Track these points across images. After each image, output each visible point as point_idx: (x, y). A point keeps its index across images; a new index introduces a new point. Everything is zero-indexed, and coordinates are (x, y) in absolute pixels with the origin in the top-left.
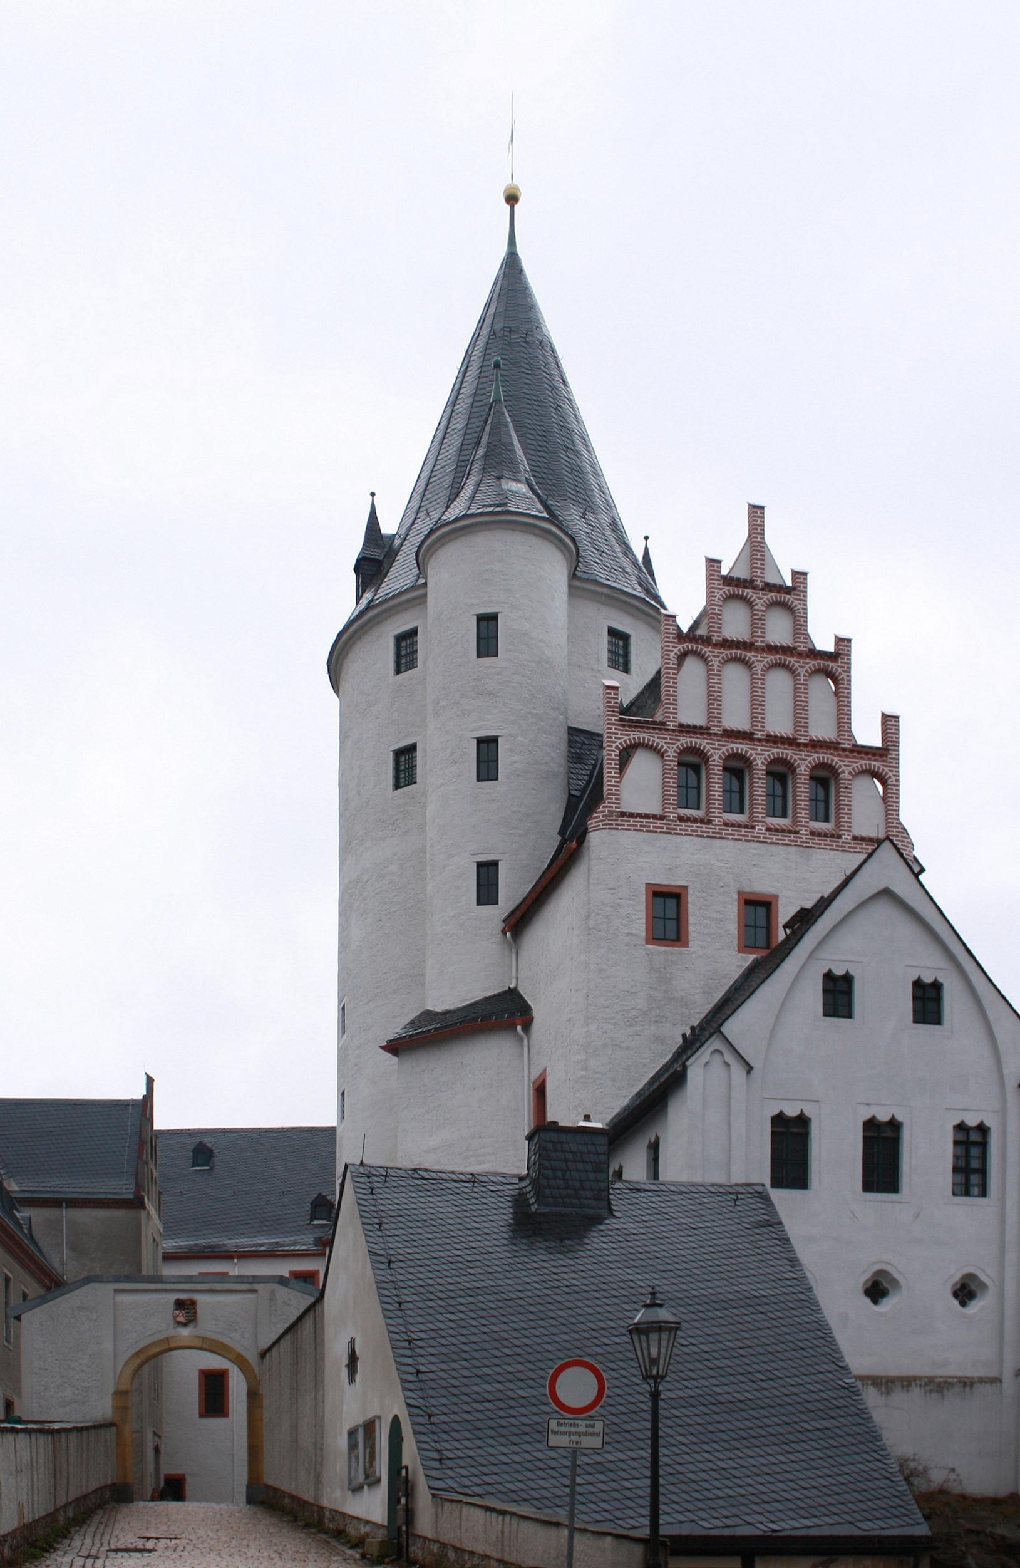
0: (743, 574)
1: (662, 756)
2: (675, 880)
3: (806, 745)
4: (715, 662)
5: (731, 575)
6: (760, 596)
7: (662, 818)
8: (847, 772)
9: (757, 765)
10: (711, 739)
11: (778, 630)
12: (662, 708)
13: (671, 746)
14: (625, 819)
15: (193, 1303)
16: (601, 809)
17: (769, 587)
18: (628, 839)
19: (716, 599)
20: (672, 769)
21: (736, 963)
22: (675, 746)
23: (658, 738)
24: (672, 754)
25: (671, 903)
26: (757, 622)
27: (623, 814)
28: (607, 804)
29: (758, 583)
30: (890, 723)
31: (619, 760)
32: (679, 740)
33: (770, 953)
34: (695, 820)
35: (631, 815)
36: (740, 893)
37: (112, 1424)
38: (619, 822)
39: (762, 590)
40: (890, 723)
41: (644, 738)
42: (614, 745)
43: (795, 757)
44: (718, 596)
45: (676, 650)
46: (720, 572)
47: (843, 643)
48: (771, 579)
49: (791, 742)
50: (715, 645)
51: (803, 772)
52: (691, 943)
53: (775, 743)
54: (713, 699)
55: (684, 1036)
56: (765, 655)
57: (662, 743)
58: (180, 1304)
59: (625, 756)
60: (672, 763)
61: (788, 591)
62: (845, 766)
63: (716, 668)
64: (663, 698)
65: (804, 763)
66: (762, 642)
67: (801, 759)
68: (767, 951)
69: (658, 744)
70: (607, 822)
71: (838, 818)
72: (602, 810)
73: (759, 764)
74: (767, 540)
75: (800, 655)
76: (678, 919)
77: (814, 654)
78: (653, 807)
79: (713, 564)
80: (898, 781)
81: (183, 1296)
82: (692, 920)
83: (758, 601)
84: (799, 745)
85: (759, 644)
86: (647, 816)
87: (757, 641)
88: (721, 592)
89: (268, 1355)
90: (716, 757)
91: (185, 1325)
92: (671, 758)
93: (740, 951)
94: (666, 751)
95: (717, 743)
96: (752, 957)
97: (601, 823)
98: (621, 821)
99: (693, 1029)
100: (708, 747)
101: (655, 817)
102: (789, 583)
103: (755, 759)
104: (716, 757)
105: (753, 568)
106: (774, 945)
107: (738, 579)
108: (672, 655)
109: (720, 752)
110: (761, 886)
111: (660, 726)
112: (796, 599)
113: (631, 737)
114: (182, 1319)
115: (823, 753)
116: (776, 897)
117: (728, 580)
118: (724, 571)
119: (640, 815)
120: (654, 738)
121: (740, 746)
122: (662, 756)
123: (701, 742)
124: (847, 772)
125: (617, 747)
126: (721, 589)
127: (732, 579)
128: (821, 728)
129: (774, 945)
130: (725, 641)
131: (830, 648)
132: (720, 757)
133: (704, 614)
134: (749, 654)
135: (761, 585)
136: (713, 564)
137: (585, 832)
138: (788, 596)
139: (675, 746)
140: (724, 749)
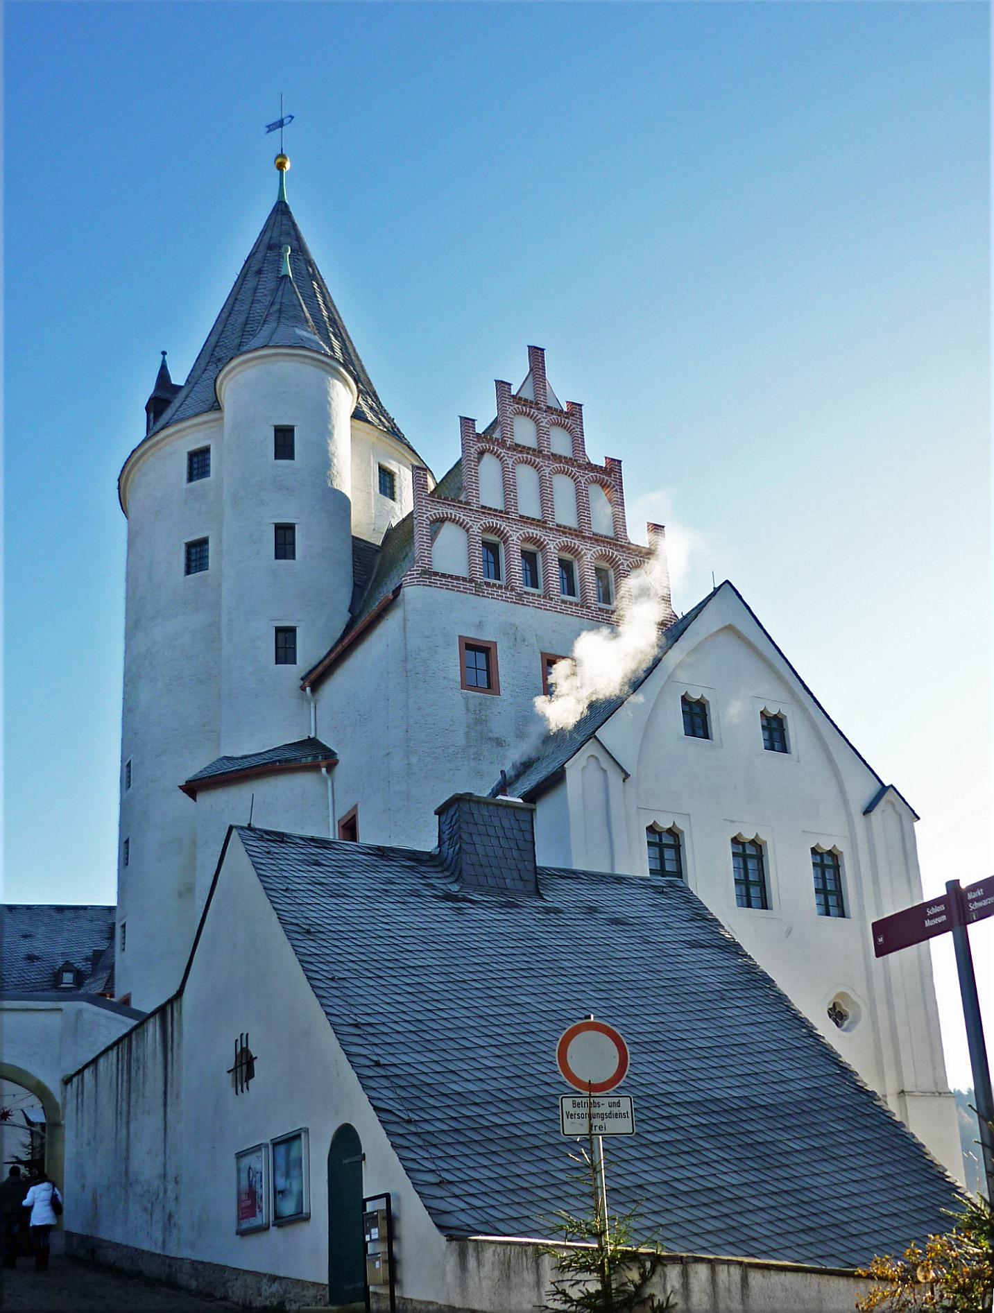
0: (528, 394)
1: (467, 531)
2: (486, 636)
4: (510, 462)
5: (519, 395)
6: (544, 416)
7: (471, 581)
8: (625, 565)
9: (550, 548)
10: (509, 523)
11: (560, 443)
12: (465, 492)
13: (475, 523)
14: (438, 578)
16: (416, 568)
19: (508, 413)
20: (477, 543)
22: (479, 524)
23: (464, 515)
24: (476, 529)
25: (481, 657)
26: (541, 433)
27: (436, 574)
28: (420, 564)
29: (542, 406)
32: (482, 520)
35: (443, 575)
36: (542, 654)
38: (432, 581)
39: (545, 412)
41: (451, 514)
42: (425, 516)
43: (581, 546)
44: (510, 410)
45: (476, 447)
46: (510, 392)
47: (614, 467)
50: (509, 449)
51: (589, 560)
52: (502, 692)
53: (564, 533)
54: (509, 488)
57: (467, 519)
60: (477, 538)
63: (510, 466)
66: (548, 451)
67: (586, 549)
69: (464, 520)
70: (421, 579)
73: (552, 548)
75: (579, 466)
76: (488, 671)
77: (591, 467)
79: (502, 386)
82: (501, 671)
83: (543, 419)
84: (584, 537)
85: (546, 453)
86: (457, 578)
87: (544, 451)
88: (512, 408)
92: (476, 533)
94: (471, 527)
95: (514, 526)
97: (416, 580)
98: (434, 579)
100: (507, 528)
101: (464, 579)
103: (548, 544)
107: (526, 400)
109: (518, 534)
112: (574, 424)
113: (440, 511)
115: (604, 546)
117: (516, 399)
118: (514, 392)
119: (451, 576)
120: (461, 515)
121: (535, 532)
122: (467, 531)
123: (502, 524)
124: (625, 565)
125: (427, 518)
126: (512, 406)
127: (520, 399)
130: (518, 445)
132: (518, 538)
133: (495, 422)
134: (538, 460)
136: (502, 386)
138: (567, 420)
139: (479, 524)
140: (521, 532)
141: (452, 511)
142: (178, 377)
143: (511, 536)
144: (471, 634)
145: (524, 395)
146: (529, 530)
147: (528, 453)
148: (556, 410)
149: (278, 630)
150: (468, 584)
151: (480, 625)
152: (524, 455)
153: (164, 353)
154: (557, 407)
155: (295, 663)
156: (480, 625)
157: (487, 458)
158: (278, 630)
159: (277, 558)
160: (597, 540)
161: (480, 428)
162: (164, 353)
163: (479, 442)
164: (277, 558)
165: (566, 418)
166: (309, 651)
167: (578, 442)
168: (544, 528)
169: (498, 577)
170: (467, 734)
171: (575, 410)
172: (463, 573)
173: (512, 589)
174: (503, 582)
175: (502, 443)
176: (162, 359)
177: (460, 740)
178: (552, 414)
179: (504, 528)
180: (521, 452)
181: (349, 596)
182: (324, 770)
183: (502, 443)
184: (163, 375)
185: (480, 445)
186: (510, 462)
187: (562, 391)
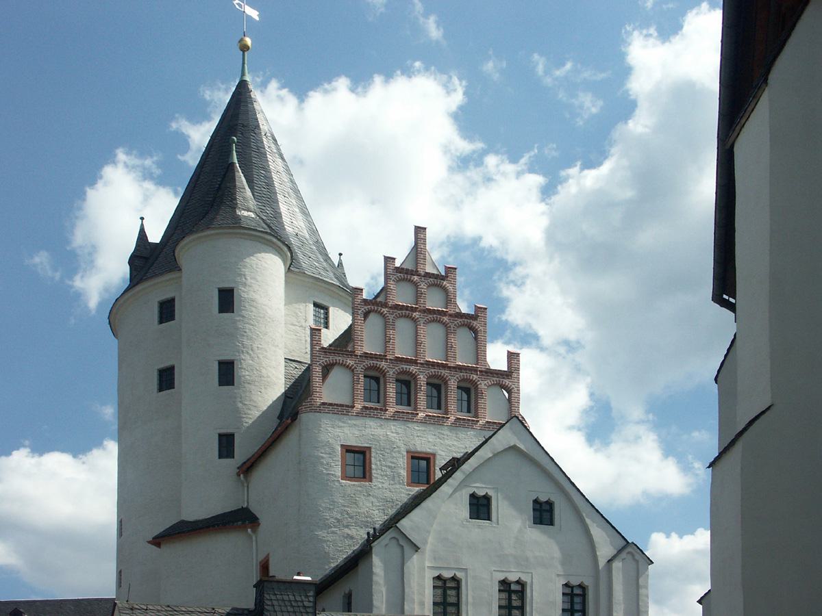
1: (353, 371)
4: (391, 317)
5: (403, 267)
11: (433, 301)
24: (359, 369)
26: (418, 295)
31: (322, 372)
34: (376, 409)
41: (339, 360)
48: (429, 269)
56: (426, 314)
61: (443, 278)
63: (391, 321)
77: (460, 315)
79: (388, 260)
86: (342, 406)
101: (347, 406)
102: (443, 274)
105: (417, 263)
107: (407, 270)
108: (360, 312)
109: (394, 370)
117: (398, 270)
118: (398, 264)
119: (337, 405)
127: (403, 269)
132: (394, 373)
135: (423, 273)
139: (362, 366)
141: (340, 358)
143: (388, 372)
146: (403, 366)
147: (407, 310)
152: (404, 312)
153: (142, 219)
157: (372, 317)
162: (142, 219)
163: (365, 305)
165: (442, 279)
167: (449, 299)
175: (385, 305)
176: (141, 223)
178: (430, 277)
179: (383, 367)
185: (366, 307)
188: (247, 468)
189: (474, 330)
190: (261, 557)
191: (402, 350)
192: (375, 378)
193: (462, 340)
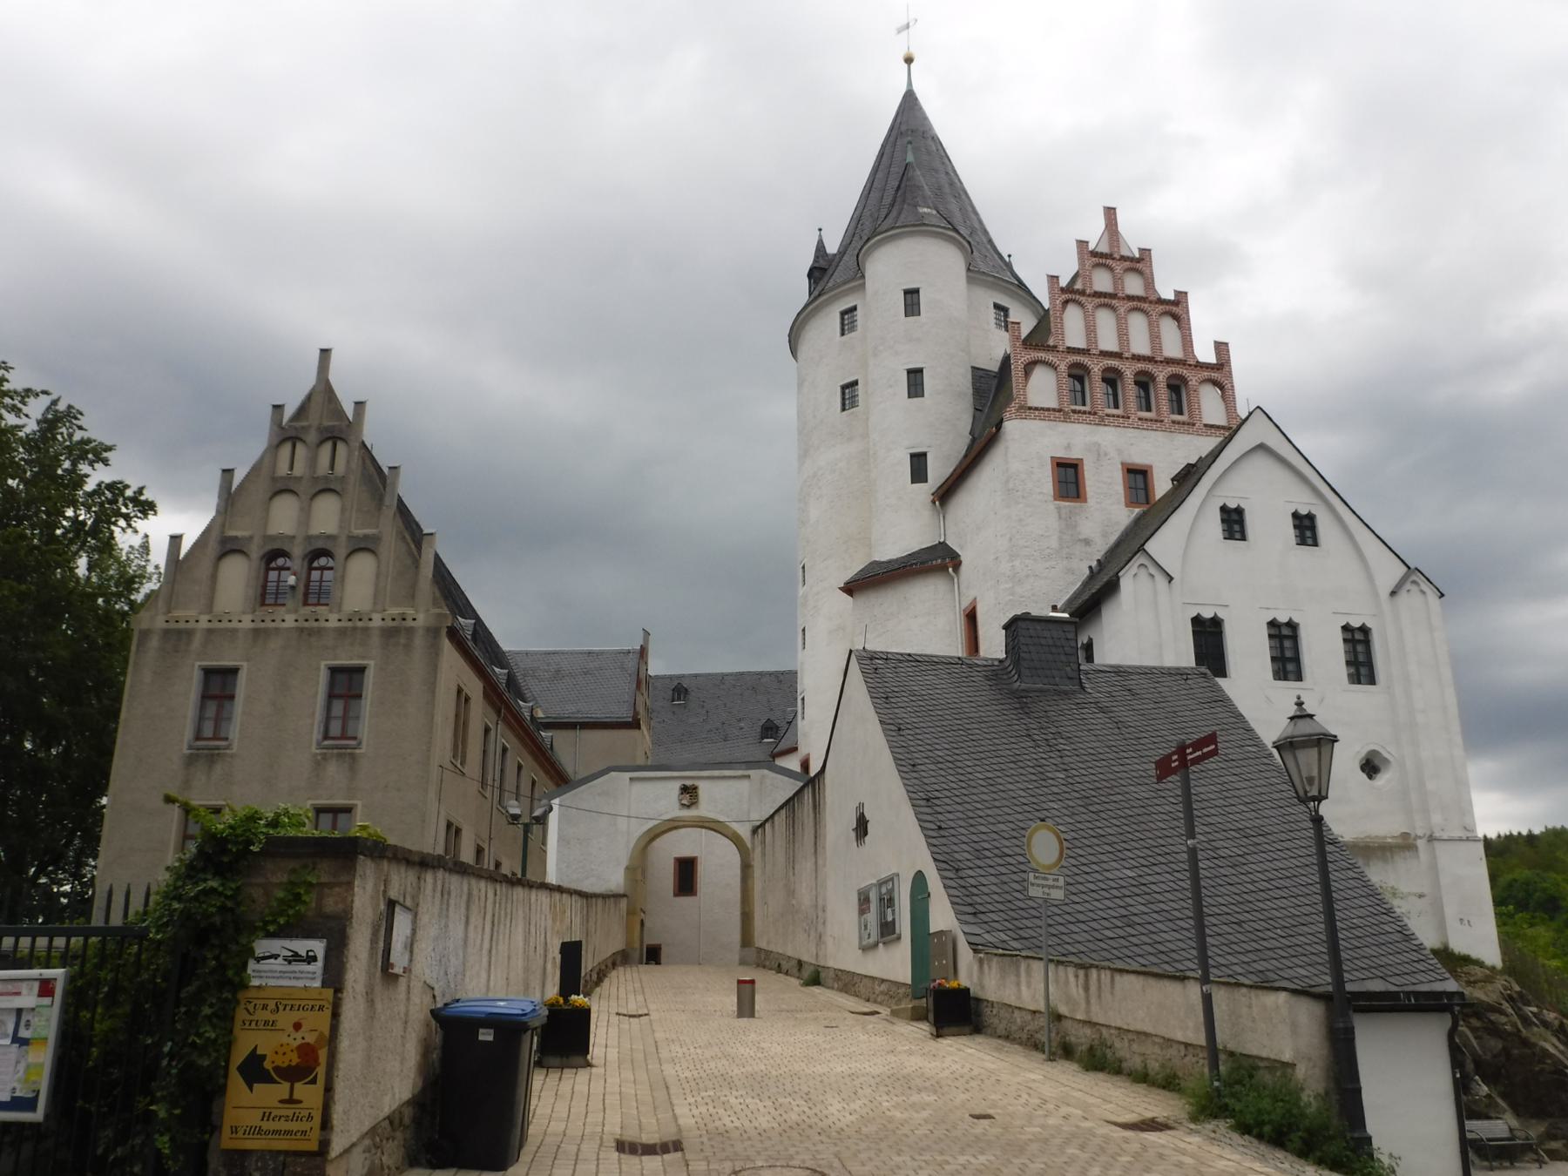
0: (1104, 249)
1: (1056, 369)
2: (1074, 455)
3: (1161, 362)
4: (1090, 307)
7: (1060, 410)
11: (1134, 286)
15: (695, 788)
17: (1123, 258)
18: (1033, 426)
21: (1123, 516)
24: (1063, 367)
25: (1071, 471)
26: (1117, 281)
27: (1030, 408)
30: (1221, 348)
33: (1149, 510)
34: (1085, 413)
35: (1036, 409)
36: (1122, 464)
37: (624, 896)
40: (1221, 348)
48: (1125, 253)
49: (1150, 359)
50: (1089, 296)
52: (1089, 500)
53: (1139, 360)
55: (1090, 567)
58: (685, 790)
59: (1029, 368)
61: (1139, 261)
62: (1193, 378)
64: (1053, 330)
65: (1162, 374)
68: (1148, 506)
71: (1190, 412)
72: (1013, 407)
74: (1119, 229)
75: (1151, 302)
77: (1161, 301)
78: (1052, 403)
79: (1082, 244)
80: (1233, 386)
81: (689, 783)
82: (1088, 483)
84: (1156, 362)
86: (1048, 410)
89: (760, 831)
90: (1096, 370)
91: (688, 807)
93: (1127, 506)
96: (1137, 510)
99: (1098, 561)
101: (1054, 410)
102: (1137, 256)
104: (1096, 370)
106: (1153, 502)
107: (1102, 253)
108: (1058, 302)
110: (1139, 459)
111: (1054, 349)
114: (684, 802)
116: (1151, 467)
117: (1094, 254)
118: (1091, 247)
119: (1043, 409)
120: (1050, 357)
122: (1056, 369)
127: (1097, 253)
128: (1172, 349)
129: (1153, 502)
131: (1172, 297)
133: (1076, 276)
135: (1118, 257)
136: (1082, 244)
137: (1001, 421)
142: (832, 248)
144: (1061, 454)
145: (1100, 249)
148: (1128, 257)
149: (913, 456)
150: (1058, 414)
151: (1068, 447)
154: (1131, 255)
155: (926, 481)
156: (1068, 447)
158: (913, 456)
159: (909, 397)
160: (1168, 363)
161: (1063, 283)
164: (909, 397)
166: (938, 471)
167: (1149, 283)
168: (1122, 358)
169: (1084, 404)
170: (1060, 539)
171: (1145, 254)
172: (1053, 404)
173: (1095, 414)
174: (1087, 408)
177: (1054, 543)
180: (1100, 297)
181: (971, 421)
182: (950, 570)
183: (1082, 293)
184: (820, 247)
186: (1090, 307)
187: (1133, 239)
188: (945, 495)
189: (1176, 317)
190: (966, 603)
191: (1108, 342)
192: (1078, 374)
193: (1168, 327)
